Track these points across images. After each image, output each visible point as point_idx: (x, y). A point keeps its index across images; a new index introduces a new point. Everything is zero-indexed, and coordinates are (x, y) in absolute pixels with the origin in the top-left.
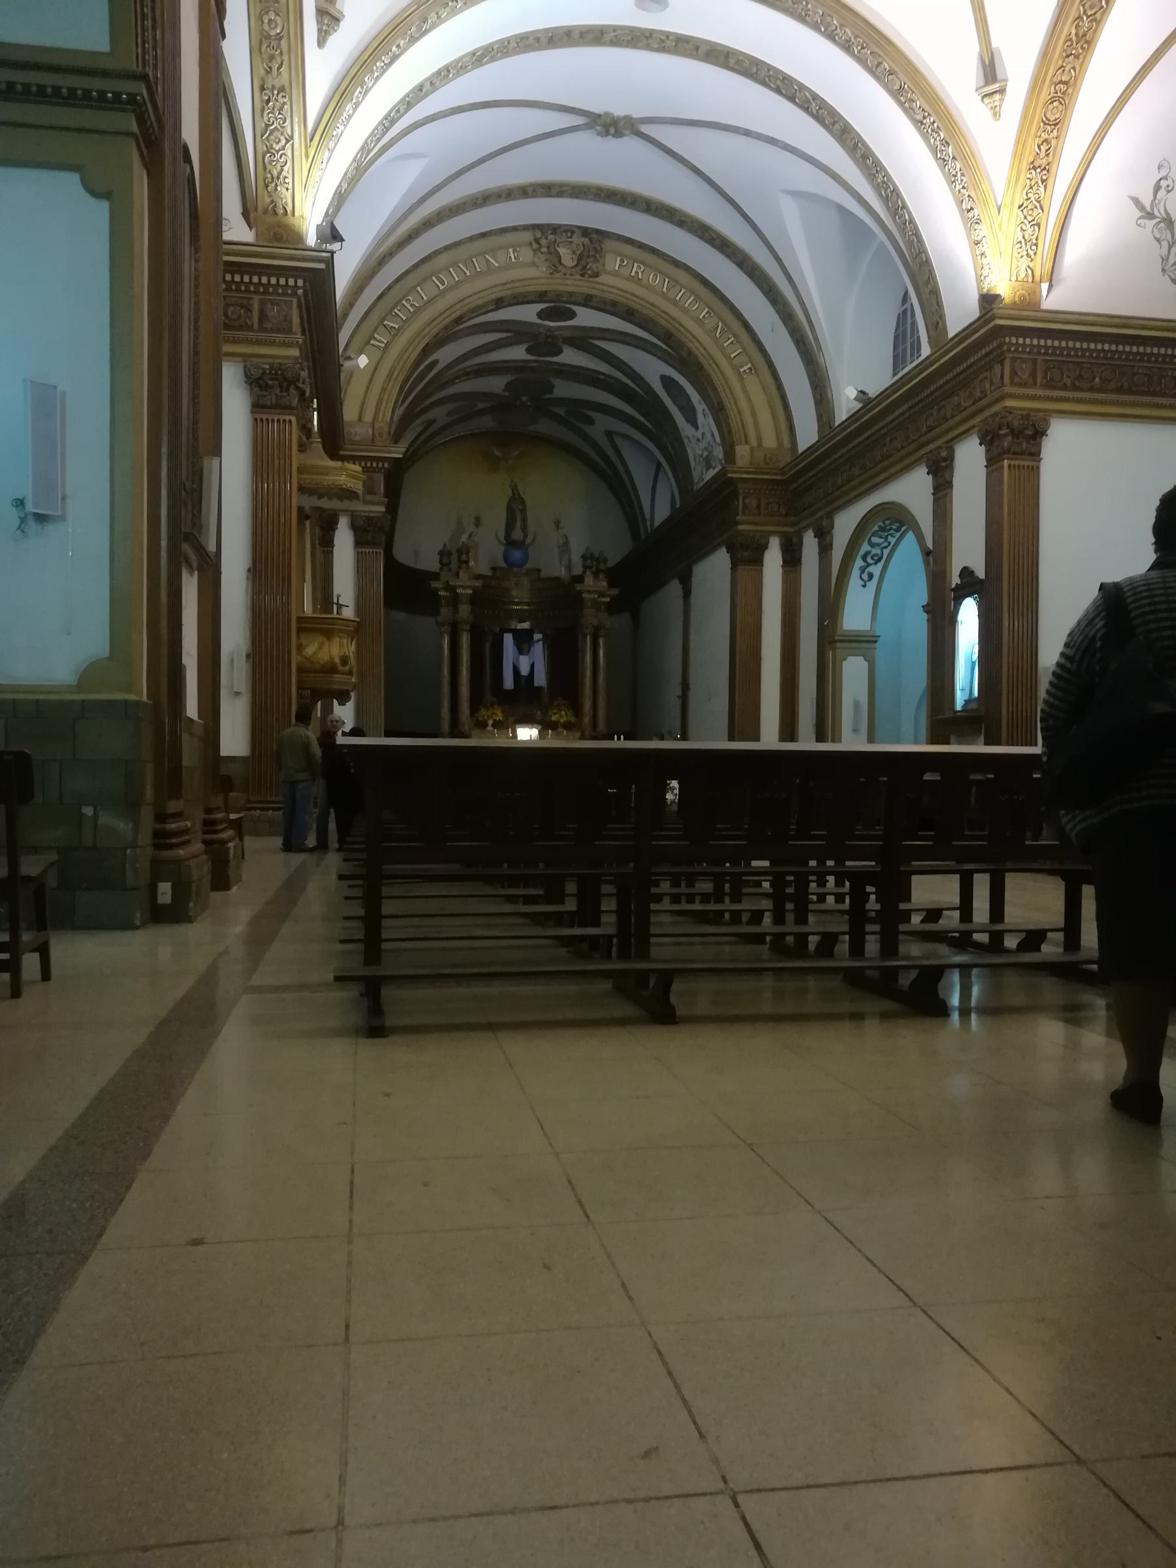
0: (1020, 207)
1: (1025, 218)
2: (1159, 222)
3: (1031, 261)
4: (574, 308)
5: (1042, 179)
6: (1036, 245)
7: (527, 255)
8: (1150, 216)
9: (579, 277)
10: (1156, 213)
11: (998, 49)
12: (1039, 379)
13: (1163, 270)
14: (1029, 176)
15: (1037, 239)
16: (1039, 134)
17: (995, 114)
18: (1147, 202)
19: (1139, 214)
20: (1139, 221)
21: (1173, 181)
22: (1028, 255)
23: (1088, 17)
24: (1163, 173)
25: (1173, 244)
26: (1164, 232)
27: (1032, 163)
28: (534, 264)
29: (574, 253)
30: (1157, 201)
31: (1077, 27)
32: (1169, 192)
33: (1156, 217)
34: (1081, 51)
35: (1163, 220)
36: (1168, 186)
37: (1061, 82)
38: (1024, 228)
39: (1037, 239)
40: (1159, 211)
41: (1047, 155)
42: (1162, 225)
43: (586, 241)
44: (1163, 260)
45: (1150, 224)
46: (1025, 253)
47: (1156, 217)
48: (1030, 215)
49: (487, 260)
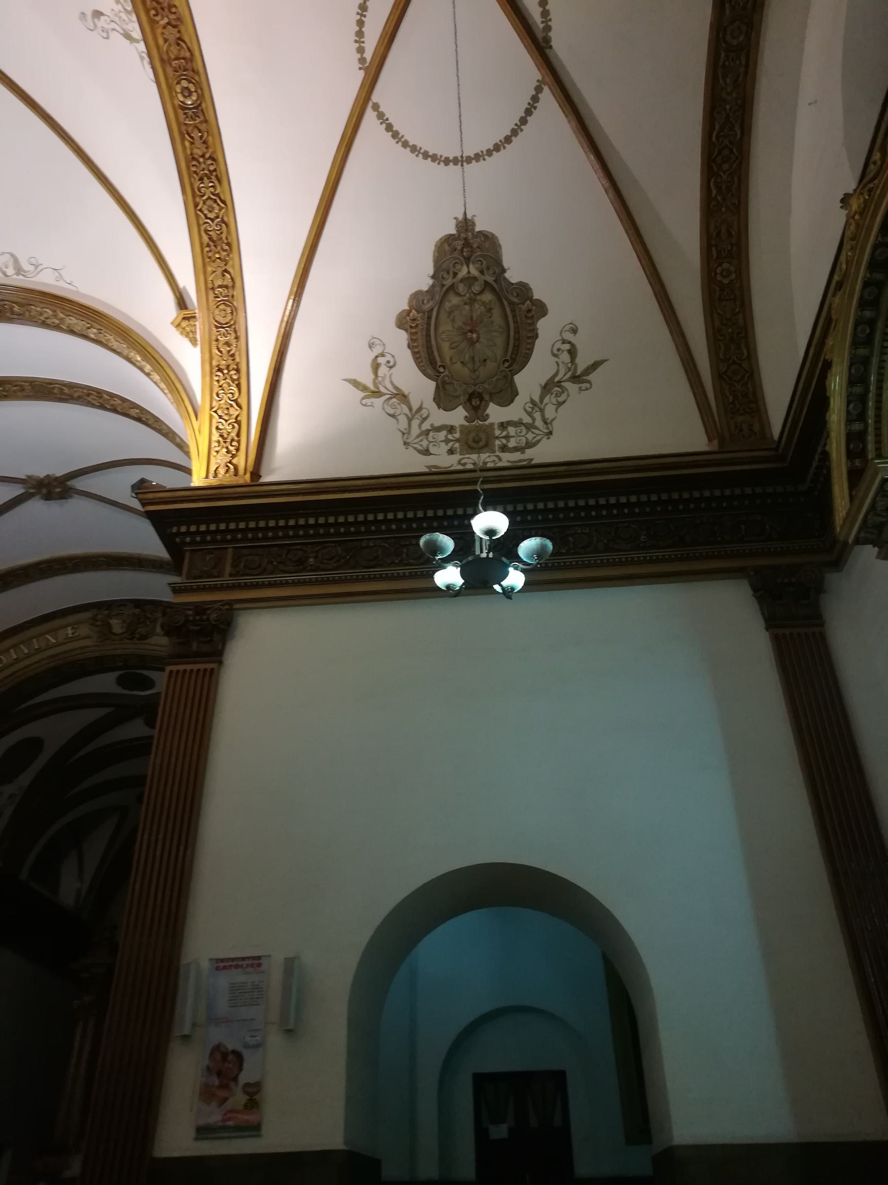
0: (211, 408)
1: (220, 417)
2: (390, 398)
3: (234, 456)
4: (146, 672)
5: (233, 380)
6: (239, 442)
7: (85, 630)
8: (377, 394)
9: (128, 641)
10: (383, 390)
11: (184, 288)
12: (228, 569)
13: (405, 443)
14: (217, 378)
15: (238, 435)
16: (214, 338)
17: (191, 341)
18: (367, 379)
19: (362, 394)
20: (364, 402)
21: (393, 357)
22: (228, 452)
23: (212, 220)
24: (378, 350)
25: (413, 416)
26: (398, 406)
27: (218, 366)
28: (88, 637)
29: (124, 622)
30: (380, 379)
31: (206, 231)
32: (391, 367)
33: (385, 394)
34: (225, 253)
35: (394, 396)
36: (388, 362)
37: (220, 287)
38: (221, 427)
39: (238, 435)
40: (385, 387)
41: (233, 355)
42: (394, 400)
43: (137, 611)
44: (403, 434)
45: (378, 402)
46: (225, 450)
47: (385, 394)
48: (226, 414)
49: (48, 640)
